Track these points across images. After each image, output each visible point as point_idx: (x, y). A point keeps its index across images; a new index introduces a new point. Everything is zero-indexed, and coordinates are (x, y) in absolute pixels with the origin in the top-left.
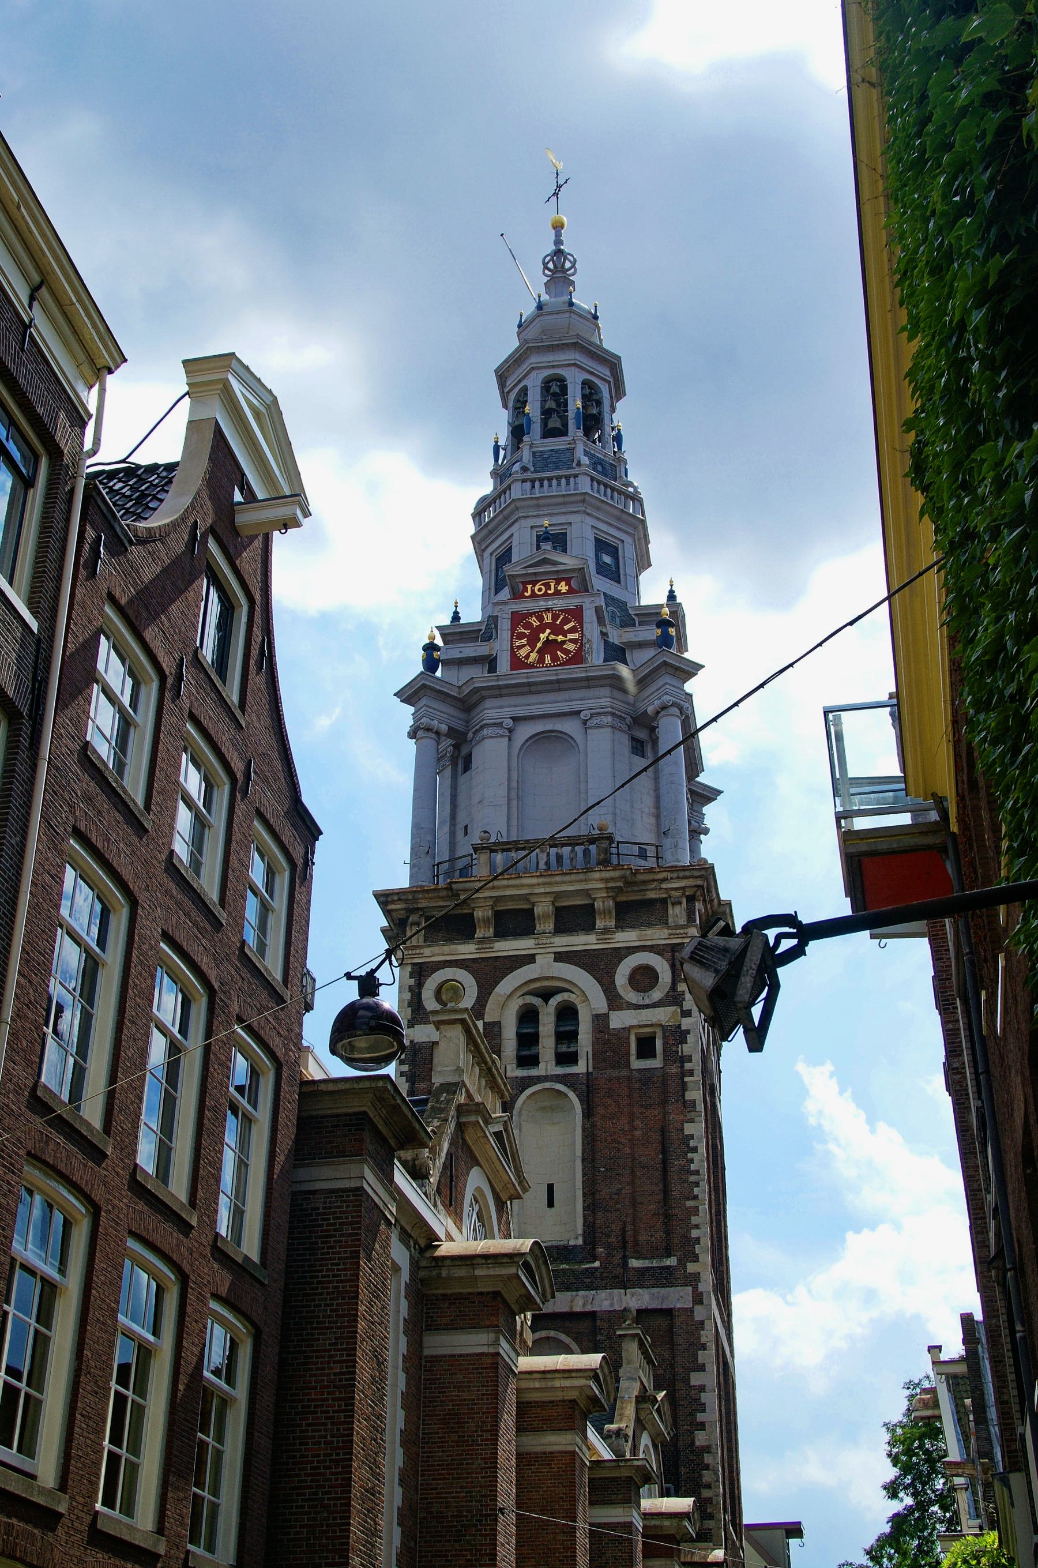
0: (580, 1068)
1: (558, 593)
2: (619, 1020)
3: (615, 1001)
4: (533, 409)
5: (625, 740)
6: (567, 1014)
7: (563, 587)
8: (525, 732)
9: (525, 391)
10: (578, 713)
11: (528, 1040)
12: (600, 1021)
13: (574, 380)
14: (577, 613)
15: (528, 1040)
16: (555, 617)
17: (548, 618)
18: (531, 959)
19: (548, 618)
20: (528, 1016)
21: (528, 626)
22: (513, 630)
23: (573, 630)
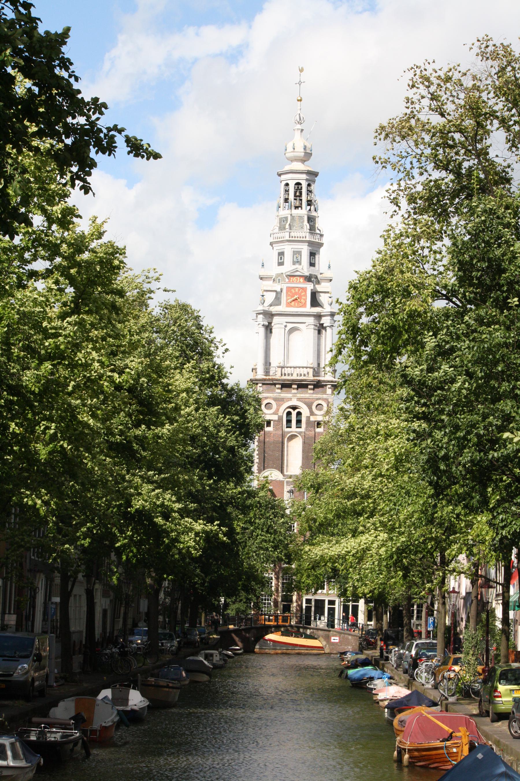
0: (303, 429)
1: (300, 282)
2: (312, 419)
3: (312, 413)
4: (291, 197)
5: (317, 331)
6: (299, 414)
7: (302, 280)
8: (290, 326)
9: (287, 185)
10: (305, 323)
11: (289, 421)
12: (308, 418)
13: (304, 184)
14: (304, 290)
15: (289, 421)
16: (299, 290)
17: (297, 290)
18: (290, 399)
19: (297, 289)
20: (289, 414)
21: (291, 292)
22: (287, 293)
23: (304, 295)
